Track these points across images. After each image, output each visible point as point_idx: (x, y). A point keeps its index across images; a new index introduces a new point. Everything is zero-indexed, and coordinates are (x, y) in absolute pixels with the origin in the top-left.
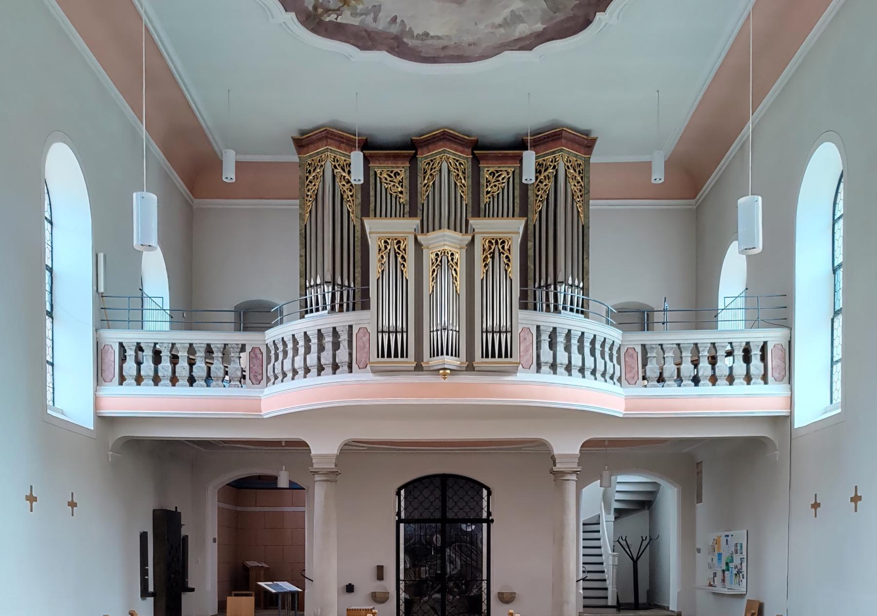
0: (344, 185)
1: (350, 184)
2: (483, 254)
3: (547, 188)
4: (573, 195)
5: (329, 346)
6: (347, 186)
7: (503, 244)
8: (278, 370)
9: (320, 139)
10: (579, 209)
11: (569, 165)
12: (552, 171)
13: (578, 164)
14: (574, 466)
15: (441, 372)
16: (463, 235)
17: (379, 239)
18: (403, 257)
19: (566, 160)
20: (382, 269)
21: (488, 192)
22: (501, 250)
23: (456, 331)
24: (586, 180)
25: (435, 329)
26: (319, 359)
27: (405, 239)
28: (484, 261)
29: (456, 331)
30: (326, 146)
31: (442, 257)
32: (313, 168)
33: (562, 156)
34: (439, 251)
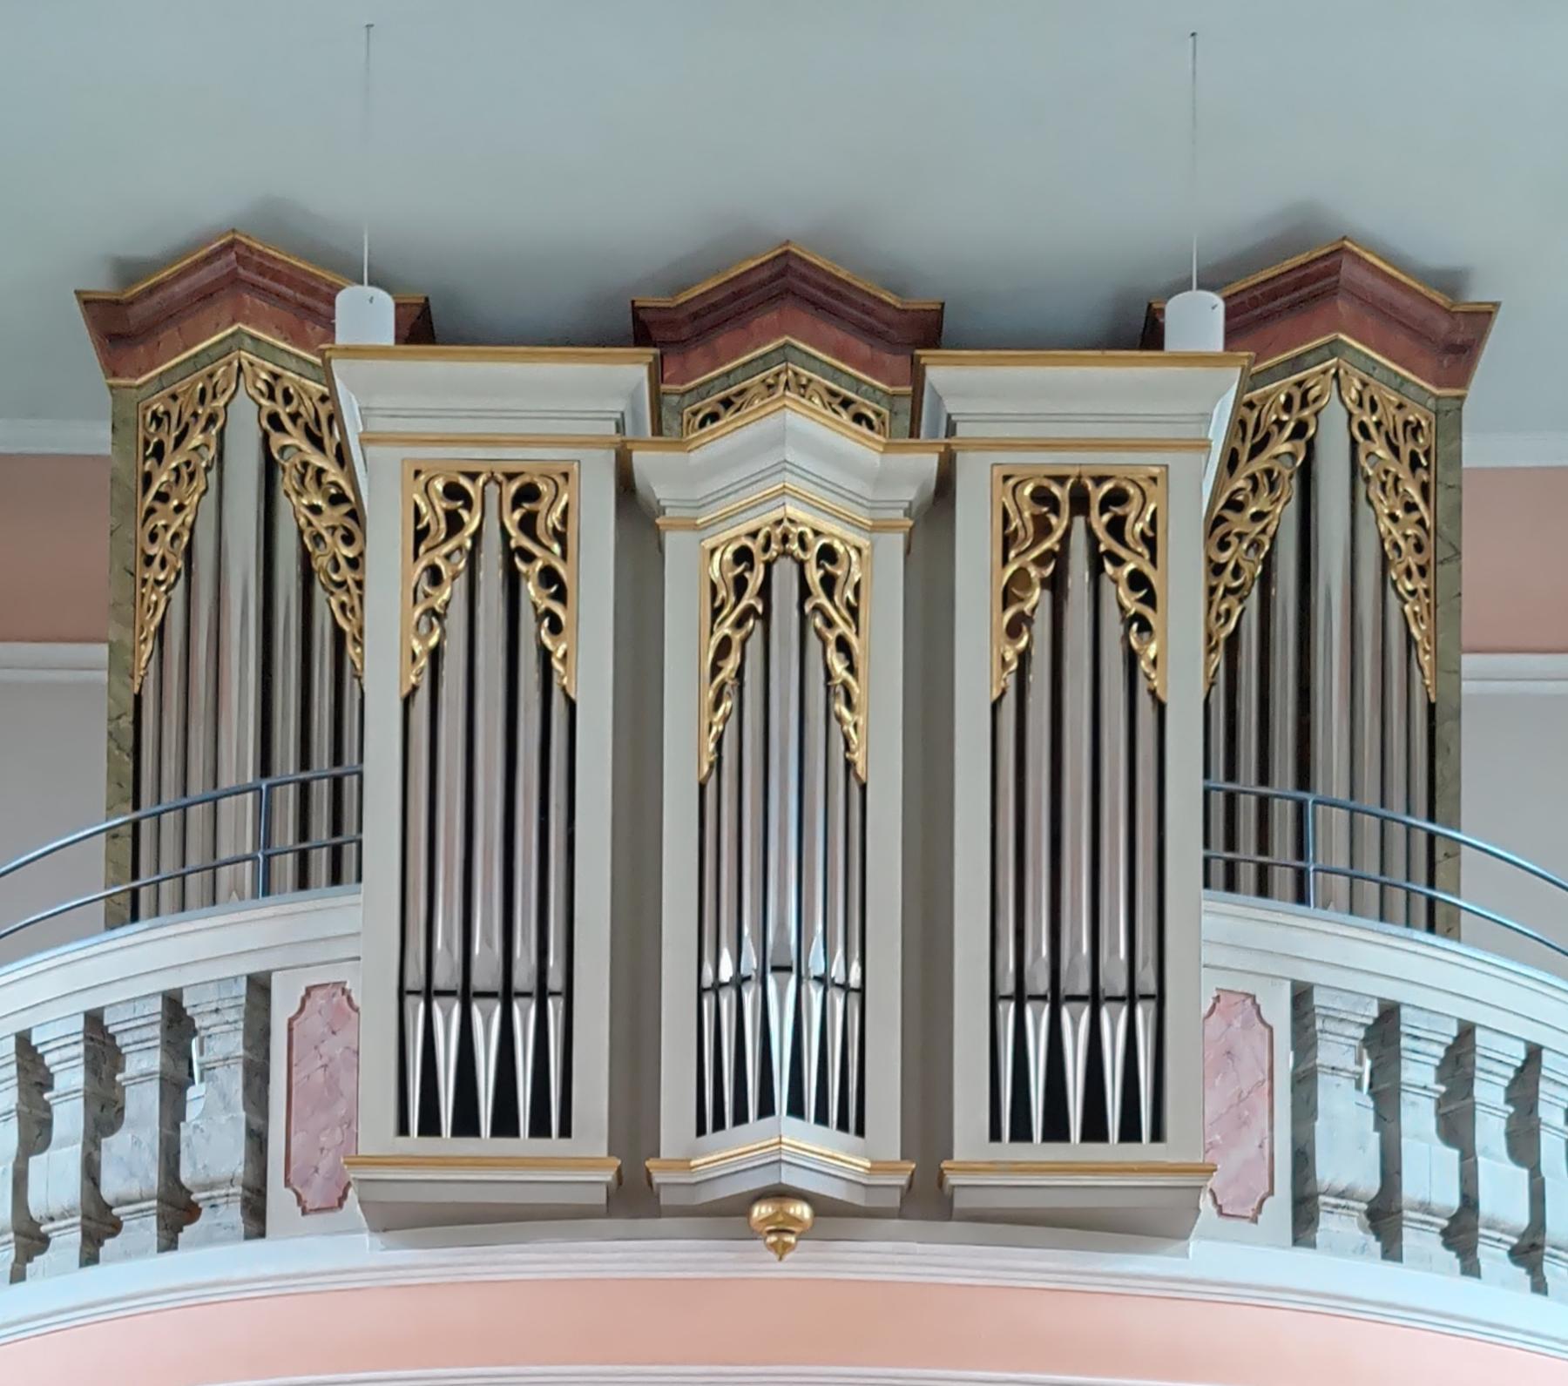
0: (315, 510)
1: (345, 508)
2: (1005, 561)
3: (1263, 531)
4: (1385, 563)
6: (334, 515)
7: (1118, 510)
9: (205, 296)
10: (1414, 630)
11: (1370, 420)
12: (1285, 448)
13: (1407, 423)
15: (761, 1211)
16: (888, 448)
17: (417, 473)
18: (549, 577)
19: (1354, 395)
20: (433, 641)
22: (1107, 543)
23: (845, 987)
24: (1442, 497)
25: (726, 973)
26: (91, 1172)
27: (566, 475)
28: (1007, 599)
29: (845, 987)
30: (233, 322)
31: (768, 566)
32: (175, 434)
33: (1336, 375)
34: (754, 535)
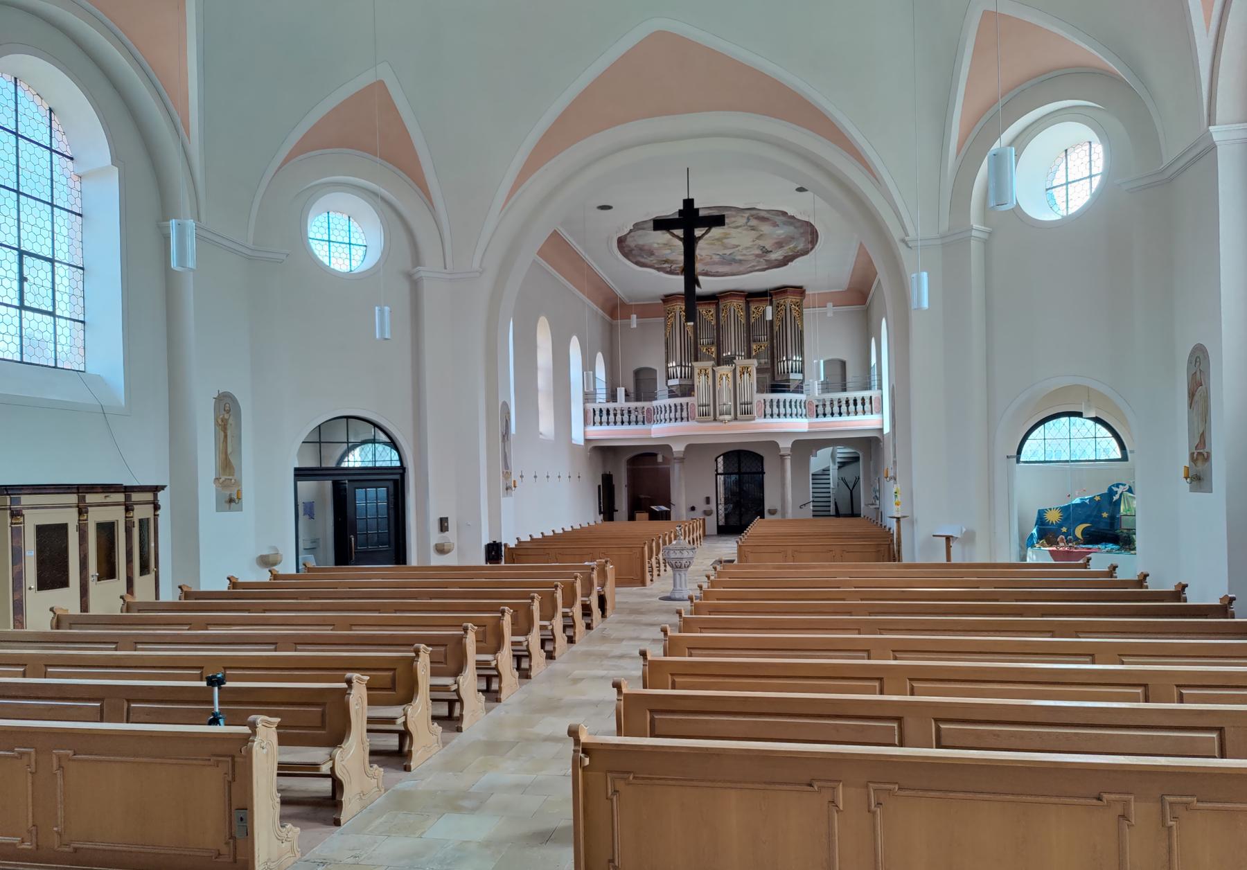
5: (679, 411)
8: (658, 418)
14: (789, 452)
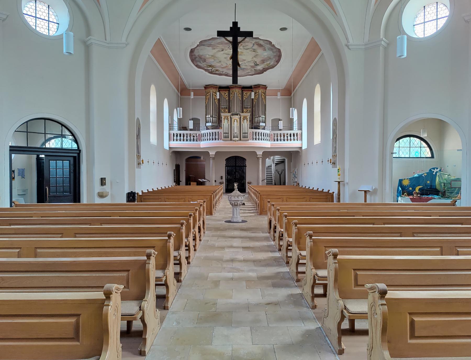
14: (261, 156)
21: (245, 97)
26: (212, 137)
